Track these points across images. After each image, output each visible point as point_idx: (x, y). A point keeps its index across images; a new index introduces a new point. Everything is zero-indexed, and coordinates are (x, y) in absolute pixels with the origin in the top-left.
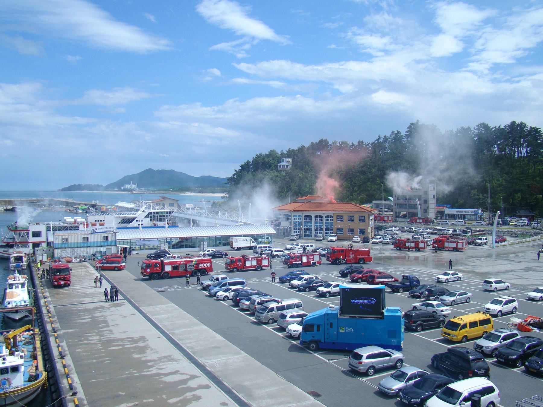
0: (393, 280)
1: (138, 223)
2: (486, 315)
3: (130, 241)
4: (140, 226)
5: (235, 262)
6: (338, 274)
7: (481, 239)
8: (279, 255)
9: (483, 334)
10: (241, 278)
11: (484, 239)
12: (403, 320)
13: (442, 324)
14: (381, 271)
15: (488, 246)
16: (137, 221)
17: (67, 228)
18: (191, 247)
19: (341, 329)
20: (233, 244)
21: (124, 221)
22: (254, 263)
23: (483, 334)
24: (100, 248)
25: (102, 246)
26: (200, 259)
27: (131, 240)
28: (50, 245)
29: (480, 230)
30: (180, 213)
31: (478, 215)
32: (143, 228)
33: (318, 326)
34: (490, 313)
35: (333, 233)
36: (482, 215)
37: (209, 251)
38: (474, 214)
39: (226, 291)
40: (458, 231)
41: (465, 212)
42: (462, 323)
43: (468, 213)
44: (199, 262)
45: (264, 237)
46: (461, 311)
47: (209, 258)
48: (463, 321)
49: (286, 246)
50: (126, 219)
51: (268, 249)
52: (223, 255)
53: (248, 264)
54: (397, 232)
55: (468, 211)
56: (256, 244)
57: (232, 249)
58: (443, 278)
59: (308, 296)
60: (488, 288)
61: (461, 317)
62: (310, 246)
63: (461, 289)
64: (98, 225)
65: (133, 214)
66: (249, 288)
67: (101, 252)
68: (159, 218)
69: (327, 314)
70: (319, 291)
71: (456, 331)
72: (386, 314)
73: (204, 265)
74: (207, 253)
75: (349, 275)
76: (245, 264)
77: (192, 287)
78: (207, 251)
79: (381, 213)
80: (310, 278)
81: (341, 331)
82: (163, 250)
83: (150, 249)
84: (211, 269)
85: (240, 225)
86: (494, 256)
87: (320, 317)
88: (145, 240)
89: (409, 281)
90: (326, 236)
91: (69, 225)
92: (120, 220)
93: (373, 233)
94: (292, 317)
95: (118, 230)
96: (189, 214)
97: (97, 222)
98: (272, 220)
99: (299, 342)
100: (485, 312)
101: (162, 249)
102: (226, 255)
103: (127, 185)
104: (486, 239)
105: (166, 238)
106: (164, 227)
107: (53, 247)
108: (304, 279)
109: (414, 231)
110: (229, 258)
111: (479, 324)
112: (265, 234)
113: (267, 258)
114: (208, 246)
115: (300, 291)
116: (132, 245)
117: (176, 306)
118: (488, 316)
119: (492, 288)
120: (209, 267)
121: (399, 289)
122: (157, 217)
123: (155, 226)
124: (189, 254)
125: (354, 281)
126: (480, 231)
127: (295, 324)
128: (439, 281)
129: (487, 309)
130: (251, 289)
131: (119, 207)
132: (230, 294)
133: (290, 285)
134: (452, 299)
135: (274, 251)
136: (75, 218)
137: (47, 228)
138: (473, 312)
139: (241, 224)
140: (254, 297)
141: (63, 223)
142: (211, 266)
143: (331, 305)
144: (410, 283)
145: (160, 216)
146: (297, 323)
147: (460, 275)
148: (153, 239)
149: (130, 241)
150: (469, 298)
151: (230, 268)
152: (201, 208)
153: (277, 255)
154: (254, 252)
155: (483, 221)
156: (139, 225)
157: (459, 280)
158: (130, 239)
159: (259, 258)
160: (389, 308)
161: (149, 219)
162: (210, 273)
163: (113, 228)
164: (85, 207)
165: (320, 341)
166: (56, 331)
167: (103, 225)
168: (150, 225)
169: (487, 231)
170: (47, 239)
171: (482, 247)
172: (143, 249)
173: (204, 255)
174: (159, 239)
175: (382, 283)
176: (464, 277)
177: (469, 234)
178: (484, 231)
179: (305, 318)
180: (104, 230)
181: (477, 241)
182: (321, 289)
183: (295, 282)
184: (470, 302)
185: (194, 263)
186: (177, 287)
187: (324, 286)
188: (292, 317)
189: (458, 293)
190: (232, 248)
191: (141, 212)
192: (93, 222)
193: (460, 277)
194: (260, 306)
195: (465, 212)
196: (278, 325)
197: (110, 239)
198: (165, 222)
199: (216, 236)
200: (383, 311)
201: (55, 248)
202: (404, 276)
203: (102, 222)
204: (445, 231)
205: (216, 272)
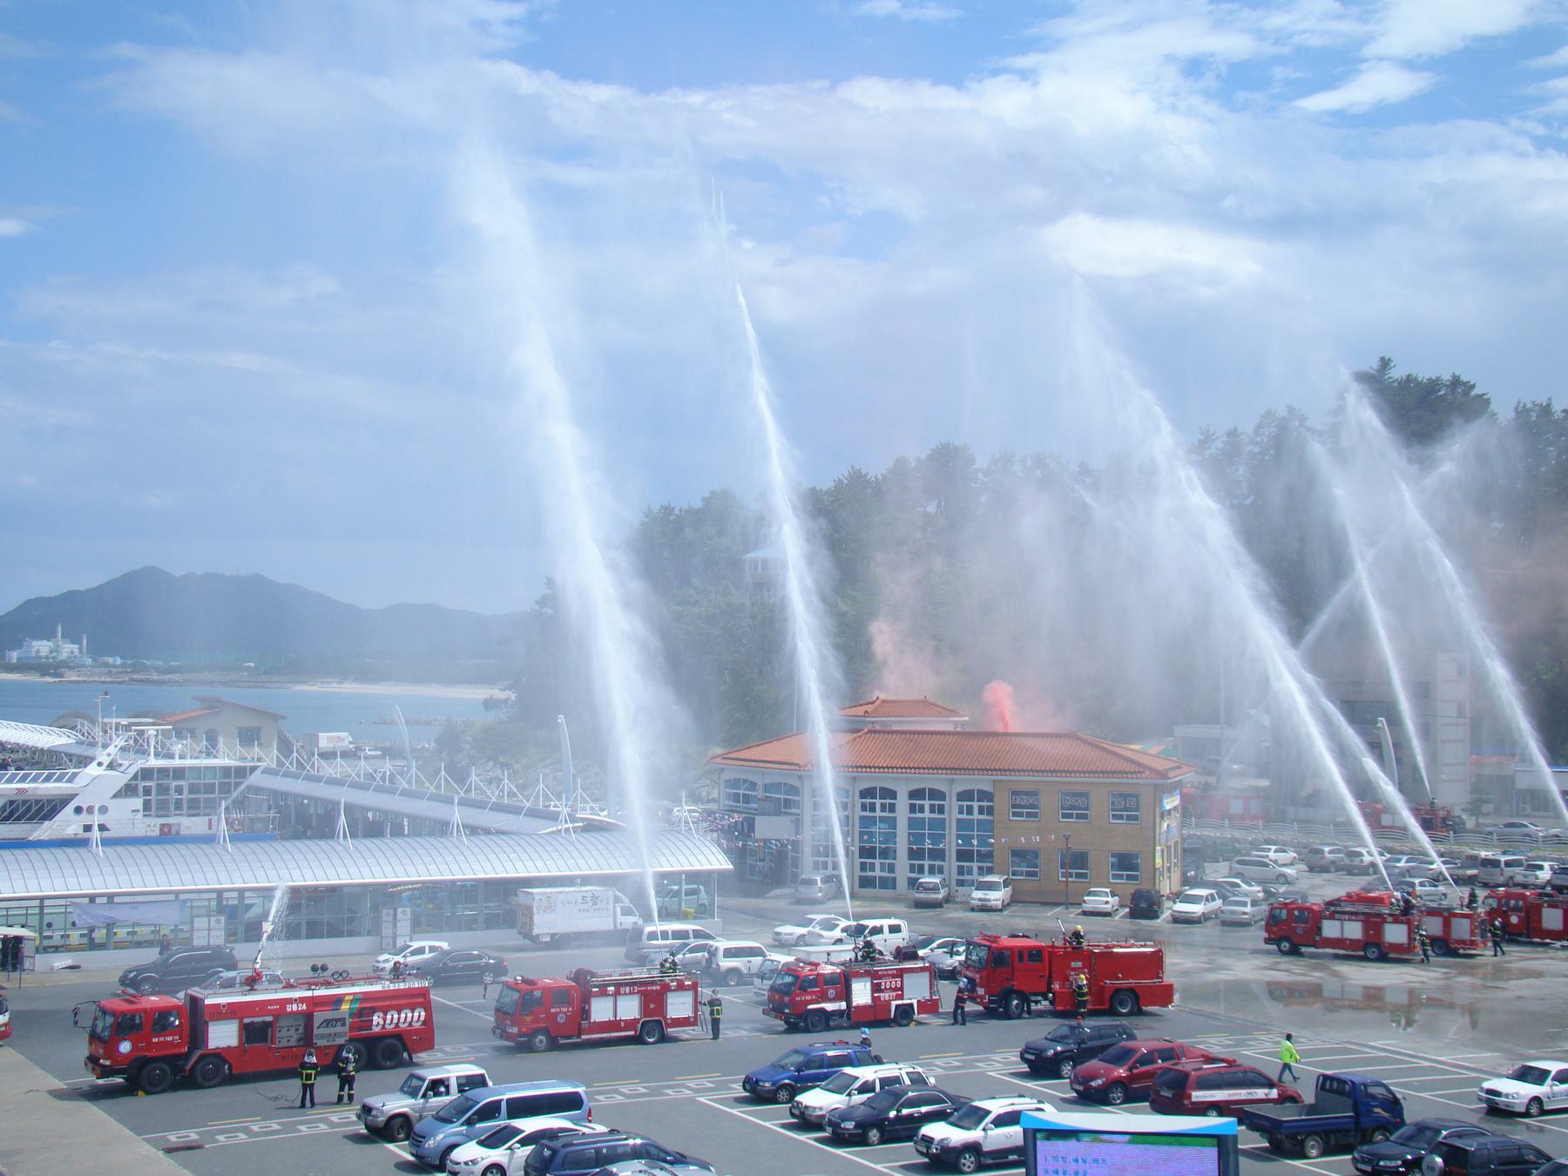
0: (1274, 1093)
1: (85, 818)
3: (42, 907)
4: (96, 834)
10: (564, 1078)
16: (78, 810)
18: (334, 932)
21: (11, 814)
26: (377, 988)
27: (47, 902)
30: (287, 775)
32: (106, 842)
35: (990, 871)
37: (420, 951)
39: (491, 1141)
44: (368, 1005)
45: (676, 888)
49: (778, 930)
50: (24, 802)
51: (693, 942)
53: (601, 1010)
54: (1289, 871)
56: (640, 922)
57: (527, 942)
58: (1519, 1092)
59: (879, 1167)
62: (886, 929)
65: (59, 780)
66: (600, 1128)
68: (186, 796)
70: (928, 1140)
73: (392, 1016)
74: (411, 959)
75: (1067, 1069)
76: (585, 1013)
77: (332, 1125)
78: (413, 953)
79: (1211, 780)
82: (203, 948)
83: (138, 945)
84: (424, 1038)
85: (567, 830)
88: (117, 899)
89: (1349, 1102)
90: (960, 883)
93: (1176, 876)
96: (331, 781)
98: (714, 807)
101: (196, 943)
102: (499, 969)
105: (220, 892)
106: (209, 839)
108: (857, 1084)
110: (512, 987)
112: (680, 873)
114: (417, 927)
115: (839, 1139)
116: (49, 925)
120: (416, 1025)
121: (1302, 1143)
122: (179, 790)
123: (167, 836)
124: (324, 968)
125: (1090, 1097)
128: (1497, 1110)
130: (612, 1132)
133: (796, 1111)
135: (721, 953)
139: (571, 825)
142: (428, 1022)
144: (1355, 1108)
148: (153, 898)
149: (42, 907)
151: (515, 1030)
152: (388, 753)
153: (734, 971)
154: (628, 956)
156: (88, 828)
158: (42, 899)
159: (653, 983)
161: (137, 803)
168: (140, 831)
172: (102, 946)
173: (397, 972)
174: (182, 897)
175: (1221, 1108)
182: (937, 1131)
183: (817, 1099)
185: (345, 1007)
186: (267, 1123)
187: (952, 1119)
191: (99, 771)
198: (215, 818)
199: (453, 882)
202: (1326, 1077)
204: (1518, 870)
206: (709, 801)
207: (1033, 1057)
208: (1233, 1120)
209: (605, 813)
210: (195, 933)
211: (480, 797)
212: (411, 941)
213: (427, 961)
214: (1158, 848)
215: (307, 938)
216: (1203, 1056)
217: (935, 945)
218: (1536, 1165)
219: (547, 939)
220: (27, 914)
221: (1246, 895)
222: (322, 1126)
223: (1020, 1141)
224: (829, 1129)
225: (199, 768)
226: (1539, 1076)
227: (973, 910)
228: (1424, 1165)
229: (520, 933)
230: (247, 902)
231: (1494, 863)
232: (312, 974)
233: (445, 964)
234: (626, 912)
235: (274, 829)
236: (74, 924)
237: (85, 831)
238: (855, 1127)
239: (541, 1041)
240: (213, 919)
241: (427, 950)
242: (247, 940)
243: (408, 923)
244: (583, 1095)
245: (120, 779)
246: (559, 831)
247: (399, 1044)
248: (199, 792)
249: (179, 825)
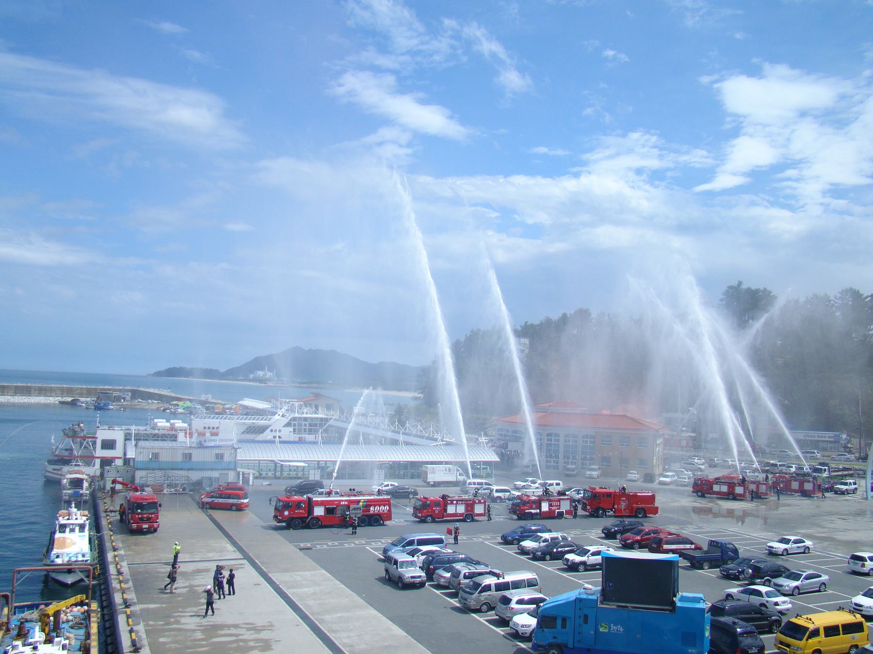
0: (693, 546)
1: (274, 434)
2: (855, 616)
3: (259, 463)
5: (429, 505)
6: (600, 534)
7: (846, 484)
8: (503, 497)
9: (850, 650)
10: (437, 532)
11: (850, 484)
12: (708, 616)
13: (776, 627)
14: (673, 531)
15: (858, 495)
16: (272, 431)
17: (158, 437)
18: (358, 478)
19: (602, 626)
20: (427, 476)
22: (461, 509)
23: (850, 650)
24: (209, 472)
25: (212, 470)
27: (261, 462)
28: (129, 464)
29: (844, 468)
30: (342, 421)
31: (841, 442)
32: (281, 442)
33: (564, 620)
34: (863, 613)
35: (593, 464)
36: (848, 443)
37: (387, 485)
38: (833, 440)
39: (412, 553)
40: (807, 469)
41: (818, 436)
42: (811, 627)
43: (823, 439)
44: (369, 504)
45: (479, 467)
46: (810, 606)
47: (386, 497)
48: (813, 623)
49: (515, 483)
50: (254, 427)
51: (485, 486)
52: (411, 492)
53: (451, 509)
54: (702, 467)
55: (823, 435)
57: (425, 484)
58: (780, 547)
59: (549, 569)
60: (858, 568)
61: (809, 616)
62: (555, 484)
63: (809, 568)
64: (208, 435)
65: (265, 420)
66: (450, 551)
67: (211, 478)
68: (307, 427)
69: (578, 600)
70: (567, 560)
71: (801, 640)
72: (679, 604)
73: (377, 508)
74: (384, 488)
75: (618, 536)
76: (446, 510)
77: (356, 544)
78: (385, 486)
79: (675, 433)
80: (552, 539)
81: (601, 630)
82: (312, 481)
83: (291, 478)
84: (388, 516)
86: (869, 513)
87: (567, 604)
89: (720, 550)
90: (582, 468)
91: (162, 432)
92: (244, 428)
93: (661, 467)
94: (520, 602)
95: (240, 445)
97: (207, 427)
98: (493, 438)
99: (530, 644)
100: (852, 609)
102: (415, 493)
103: (258, 372)
104: (855, 484)
105: (319, 462)
106: (315, 443)
107: (134, 467)
108: (542, 539)
109: (730, 466)
111: (843, 630)
112: (481, 461)
113: (482, 501)
115: (535, 558)
116: (262, 470)
117: (329, 575)
118: (859, 618)
119: (866, 570)
120: (386, 511)
121: (702, 564)
122: (305, 425)
123: (301, 441)
124: (354, 490)
125: (626, 546)
126: (845, 469)
127: (526, 615)
128: (772, 553)
129: (856, 604)
130: (454, 552)
131: (246, 407)
132: (420, 559)
133: (520, 548)
134: (795, 583)
135: (494, 491)
136: (172, 421)
137: (126, 436)
138: (830, 608)
139: (442, 443)
140: (458, 566)
141: (153, 428)
142: (390, 510)
143: (586, 585)
144: (722, 552)
145: (310, 425)
146: (528, 614)
147: (808, 543)
149: (259, 463)
150: (824, 584)
153: (499, 497)
154: (461, 491)
155: (850, 452)
156: (275, 437)
157: (806, 552)
158: (259, 460)
159: (470, 500)
160: (685, 594)
161: (291, 429)
162: (387, 523)
163: (232, 440)
164: (188, 404)
165: (566, 646)
166: (129, 605)
167: (217, 434)
168: (292, 439)
169: (856, 470)
170: (125, 454)
171: (847, 497)
172: (279, 478)
173: (379, 492)
175: (674, 551)
176: (815, 548)
177: (825, 475)
178: (850, 469)
179: (542, 604)
180: (218, 443)
181: (839, 486)
182: (571, 557)
183: (528, 544)
184: (825, 591)
186: (333, 542)
187: (576, 553)
188: (520, 602)
189: (804, 574)
190: (425, 482)
192: (201, 429)
193: (808, 548)
194: (467, 581)
195: (818, 436)
196: (497, 615)
197: (227, 458)
198: (317, 436)
199: (400, 462)
200: (674, 599)
201: (137, 469)
202: (712, 541)
203: (215, 430)
204: (784, 468)
205: (396, 520)
206: (492, 436)
207: (606, 532)
208: (677, 555)
209: (453, 439)
210: (310, 476)
211: (409, 432)
212: (384, 481)
213: (389, 489)
214: (655, 457)
215: (348, 479)
216: (668, 532)
217: (572, 490)
218: (784, 572)
219: (433, 483)
220: (254, 466)
221: (686, 475)
222: (353, 544)
223: (601, 561)
224: (532, 555)
225: (311, 418)
226: (787, 541)
227: (586, 478)
228: (745, 572)
229: (423, 481)
230: (328, 465)
231: (776, 465)
232: (349, 492)
233: (396, 491)
234: (460, 475)
235: (337, 440)
236: (270, 470)
237: (274, 438)
238: (541, 554)
239: (429, 519)
240: (316, 471)
241: (390, 485)
242: (327, 479)
243: (383, 476)
244: (444, 539)
245: (285, 421)
246: (438, 445)
247: (380, 519)
248: (312, 426)
249: (305, 437)
